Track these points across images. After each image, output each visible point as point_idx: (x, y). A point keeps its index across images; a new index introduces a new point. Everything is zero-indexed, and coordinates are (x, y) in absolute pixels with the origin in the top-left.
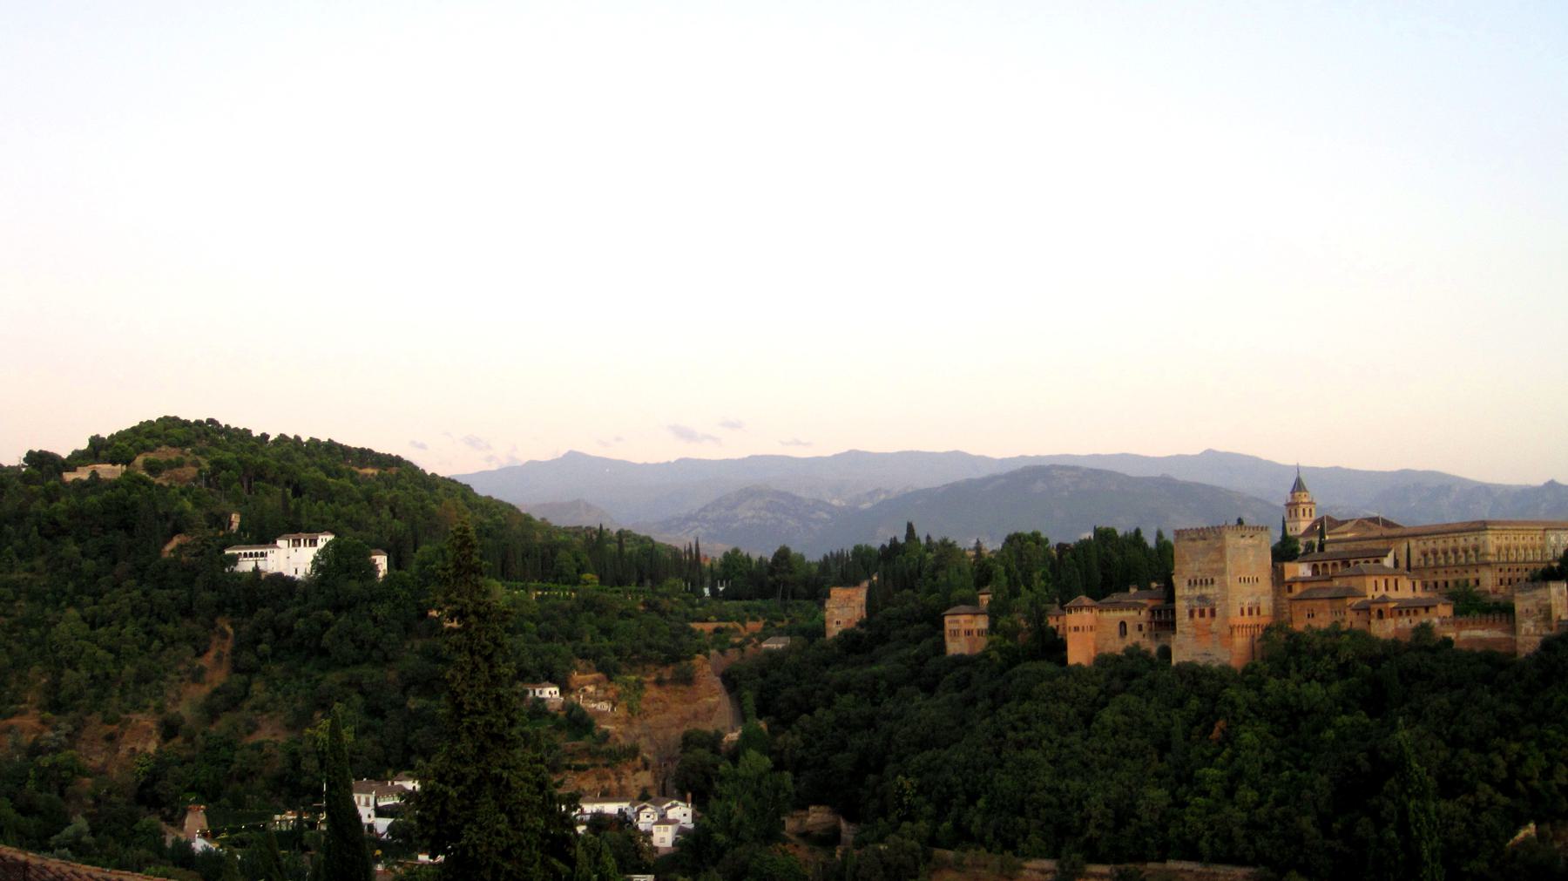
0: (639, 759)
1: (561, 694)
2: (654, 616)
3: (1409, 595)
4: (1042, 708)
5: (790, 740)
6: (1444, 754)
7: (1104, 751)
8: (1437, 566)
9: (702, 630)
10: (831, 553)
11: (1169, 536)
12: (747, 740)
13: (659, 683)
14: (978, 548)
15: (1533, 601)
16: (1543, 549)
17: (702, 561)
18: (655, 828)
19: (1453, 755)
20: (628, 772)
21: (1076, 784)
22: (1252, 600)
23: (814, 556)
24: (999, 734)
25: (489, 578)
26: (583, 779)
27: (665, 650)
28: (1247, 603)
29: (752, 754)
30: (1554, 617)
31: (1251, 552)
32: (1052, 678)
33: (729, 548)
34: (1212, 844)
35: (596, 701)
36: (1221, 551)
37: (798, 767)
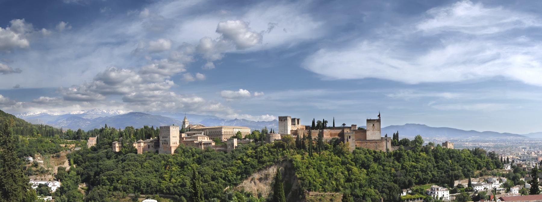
0: (49, 172)
1: (33, 159)
2: (52, 143)
3: (207, 141)
4: (132, 163)
5: (80, 169)
6: (213, 172)
7: (144, 172)
8: (212, 135)
9: (62, 146)
10: (90, 130)
11: (159, 128)
12: (71, 169)
13: (53, 157)
14: (120, 130)
15: (230, 142)
16: (233, 132)
17: (63, 132)
18: (52, 187)
19: (214, 172)
20: (46, 175)
21: (139, 178)
22: (175, 141)
23: (86, 131)
24: (124, 168)
25: (19, 135)
26: (37, 176)
27: (55, 150)
28: (174, 141)
29: (72, 172)
30: (234, 146)
31: (175, 131)
32: (134, 156)
33: (68, 129)
34: (166, 190)
35: (40, 160)
36: (169, 131)
37: (82, 175)
